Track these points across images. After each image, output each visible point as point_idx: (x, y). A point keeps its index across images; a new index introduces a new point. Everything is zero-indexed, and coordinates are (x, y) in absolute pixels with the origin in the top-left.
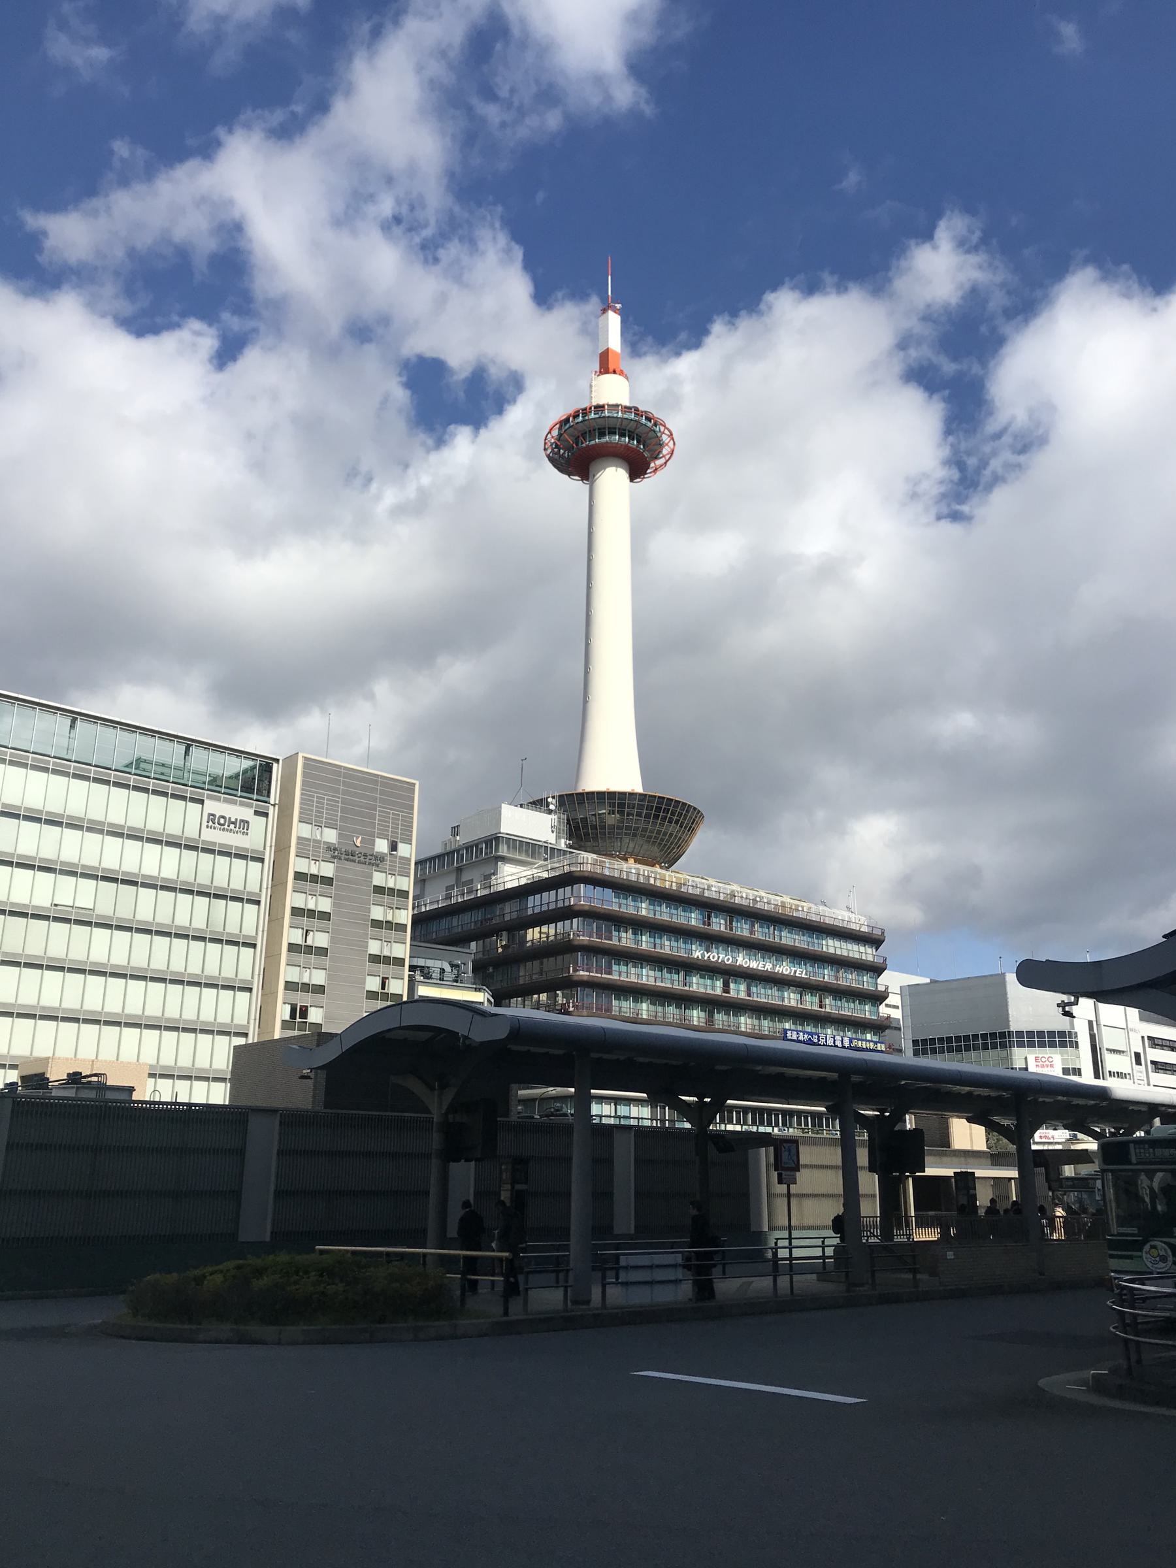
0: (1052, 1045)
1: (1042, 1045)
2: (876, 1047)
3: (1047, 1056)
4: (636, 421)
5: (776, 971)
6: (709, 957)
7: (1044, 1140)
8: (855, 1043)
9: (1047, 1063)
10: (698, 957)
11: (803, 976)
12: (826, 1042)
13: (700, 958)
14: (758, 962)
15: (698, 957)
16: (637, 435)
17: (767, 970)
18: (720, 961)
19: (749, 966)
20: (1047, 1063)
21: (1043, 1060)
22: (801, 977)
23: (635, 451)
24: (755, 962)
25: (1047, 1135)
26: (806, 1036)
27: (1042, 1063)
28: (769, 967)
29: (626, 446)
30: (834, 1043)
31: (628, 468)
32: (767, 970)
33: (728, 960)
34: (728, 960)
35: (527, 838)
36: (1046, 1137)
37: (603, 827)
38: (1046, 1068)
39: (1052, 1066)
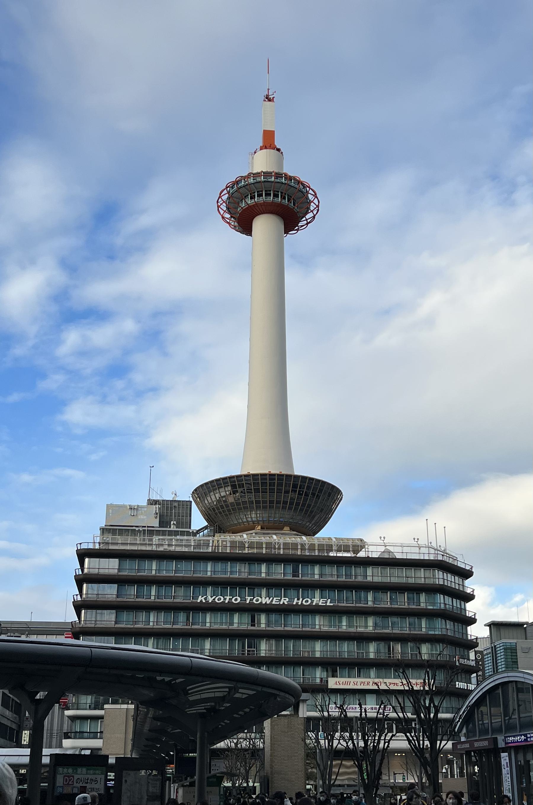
4: (286, 184)
5: (294, 603)
6: (214, 599)
10: (201, 601)
11: (328, 604)
13: (204, 601)
14: (271, 598)
15: (201, 601)
16: (288, 195)
17: (284, 603)
18: (227, 602)
19: (261, 603)
23: (286, 208)
24: (268, 598)
28: (285, 601)
29: (280, 205)
32: (284, 603)
33: (236, 600)
34: (236, 600)
35: (132, 526)
37: (227, 506)
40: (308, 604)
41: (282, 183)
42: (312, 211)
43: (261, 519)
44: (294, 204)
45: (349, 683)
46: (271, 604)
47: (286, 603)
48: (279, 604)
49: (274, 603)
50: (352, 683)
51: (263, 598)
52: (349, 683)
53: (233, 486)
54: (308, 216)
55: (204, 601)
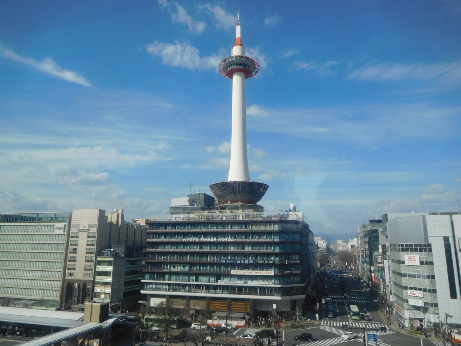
0: (416, 250)
1: (412, 250)
2: (269, 262)
3: (413, 256)
7: (412, 295)
8: (256, 261)
9: (413, 259)
12: (240, 262)
18: (194, 240)
20: (413, 259)
21: (411, 257)
22: (231, 241)
25: (413, 293)
26: (230, 261)
27: (410, 259)
28: (215, 239)
30: (245, 262)
31: (245, 76)
32: (215, 241)
36: (413, 294)
38: (412, 261)
39: (415, 261)
40: (224, 240)
41: (243, 60)
42: (257, 68)
43: (233, 197)
44: (248, 67)
45: (238, 272)
46: (210, 241)
47: (216, 240)
48: (213, 241)
49: (211, 240)
50: (240, 272)
51: (207, 239)
52: (238, 272)
53: (219, 187)
54: (256, 70)
55: (185, 240)
